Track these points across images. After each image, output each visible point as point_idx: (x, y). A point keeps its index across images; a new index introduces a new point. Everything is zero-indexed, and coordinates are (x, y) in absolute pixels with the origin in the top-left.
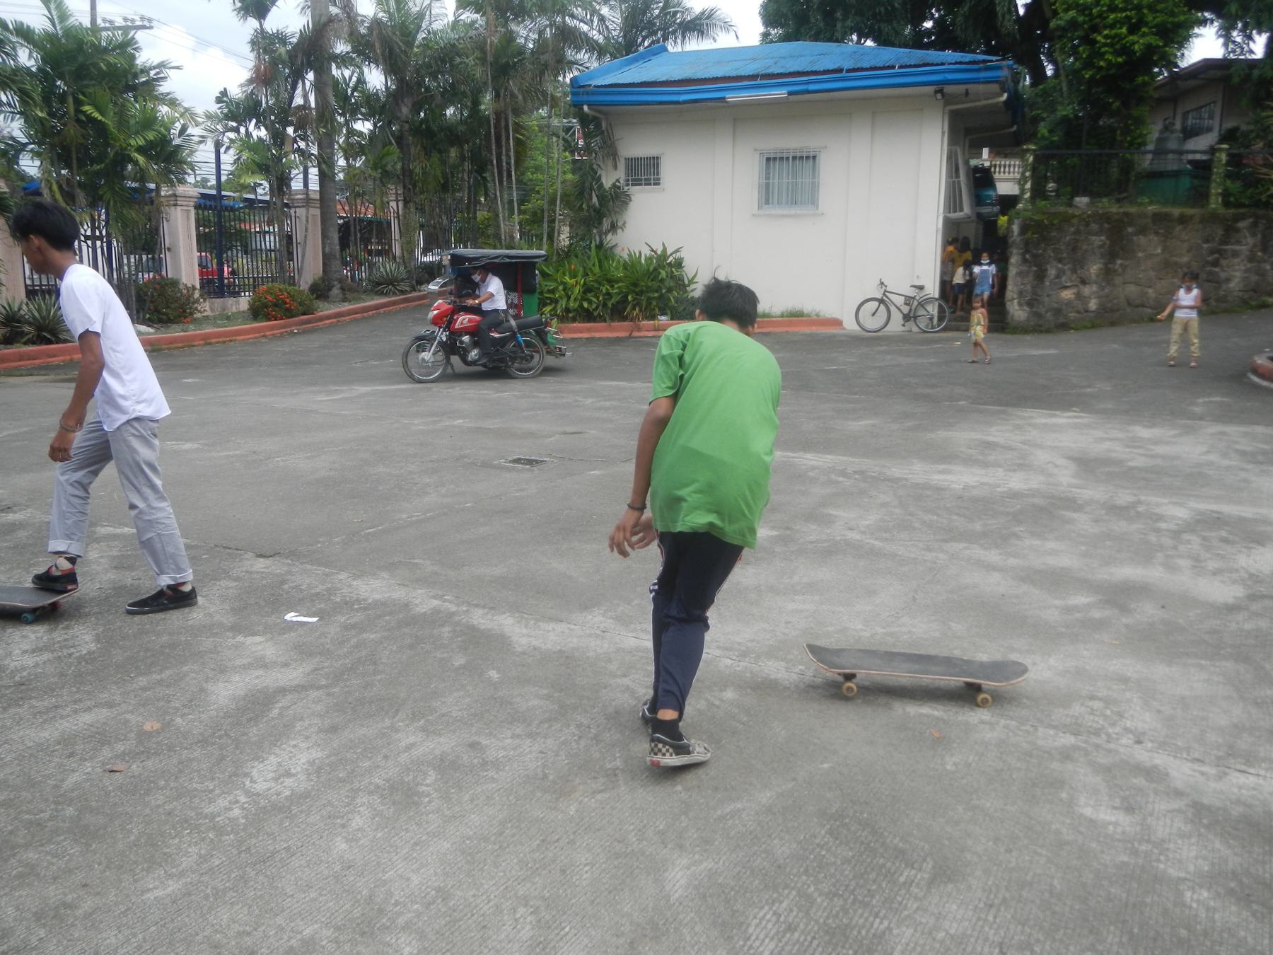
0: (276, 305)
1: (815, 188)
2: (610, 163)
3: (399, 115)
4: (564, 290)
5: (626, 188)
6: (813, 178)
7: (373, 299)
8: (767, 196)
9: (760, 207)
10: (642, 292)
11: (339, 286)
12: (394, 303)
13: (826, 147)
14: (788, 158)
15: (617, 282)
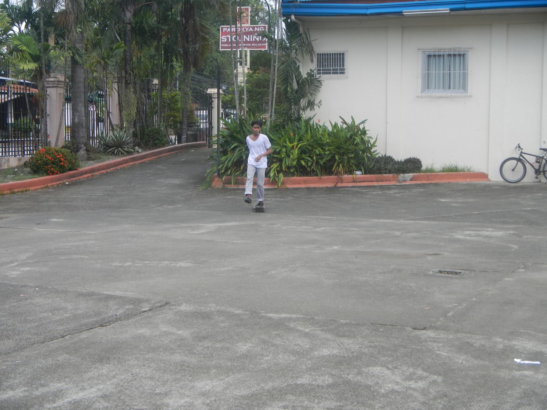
0: (53, 163)
1: (465, 77)
2: (308, 57)
3: (125, 18)
4: (286, 152)
5: (318, 76)
6: (464, 69)
7: (109, 159)
8: (427, 84)
9: (423, 91)
10: (344, 154)
11: (85, 148)
12: (126, 161)
13: (471, 49)
14: (444, 55)
15: (325, 146)
